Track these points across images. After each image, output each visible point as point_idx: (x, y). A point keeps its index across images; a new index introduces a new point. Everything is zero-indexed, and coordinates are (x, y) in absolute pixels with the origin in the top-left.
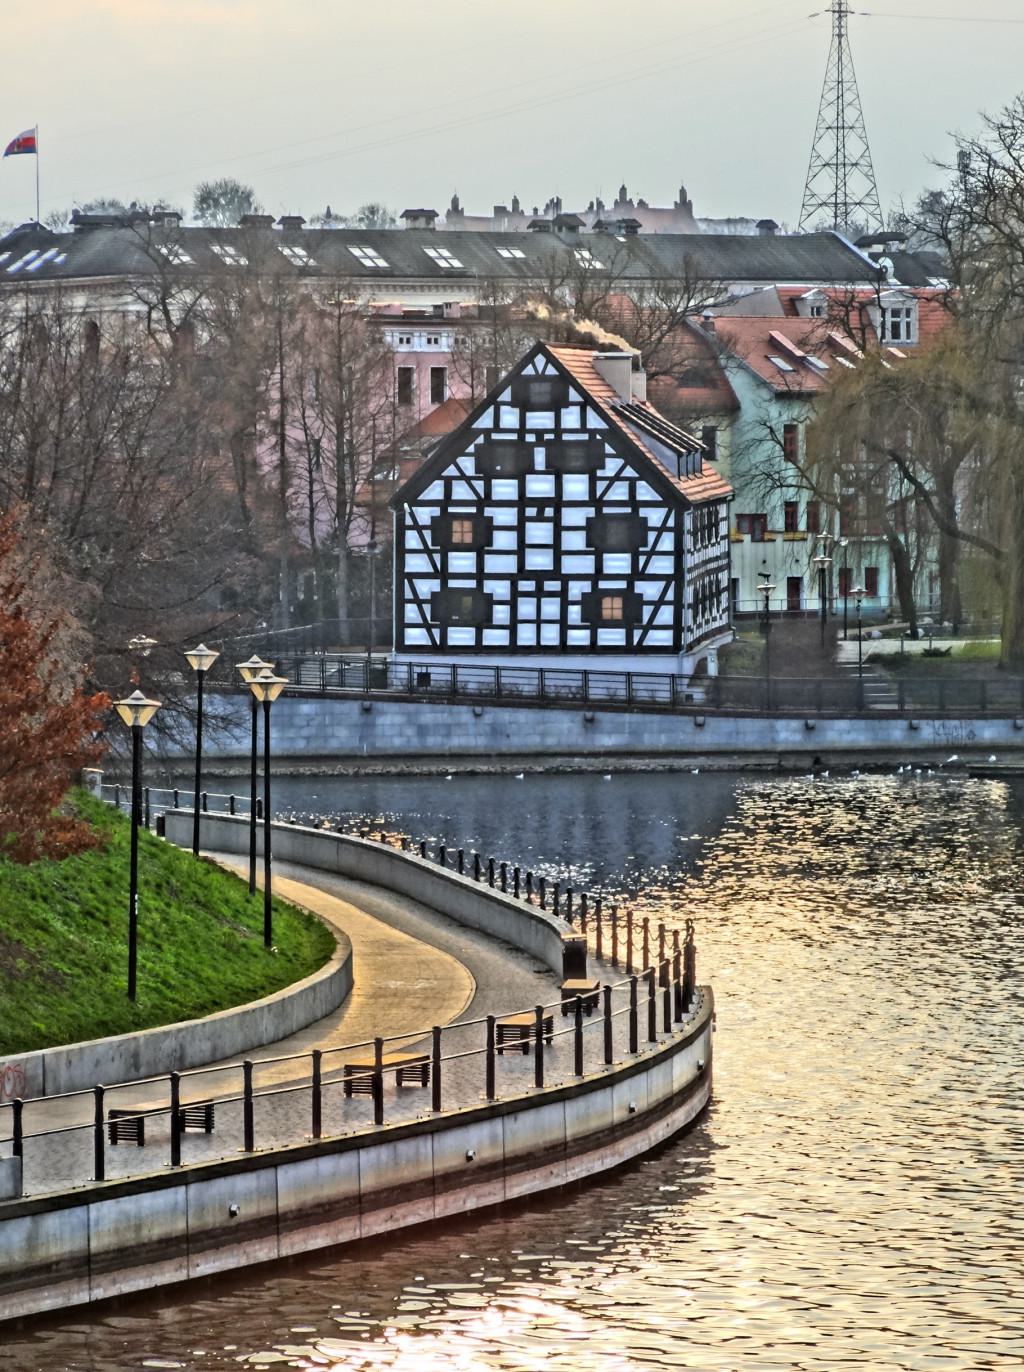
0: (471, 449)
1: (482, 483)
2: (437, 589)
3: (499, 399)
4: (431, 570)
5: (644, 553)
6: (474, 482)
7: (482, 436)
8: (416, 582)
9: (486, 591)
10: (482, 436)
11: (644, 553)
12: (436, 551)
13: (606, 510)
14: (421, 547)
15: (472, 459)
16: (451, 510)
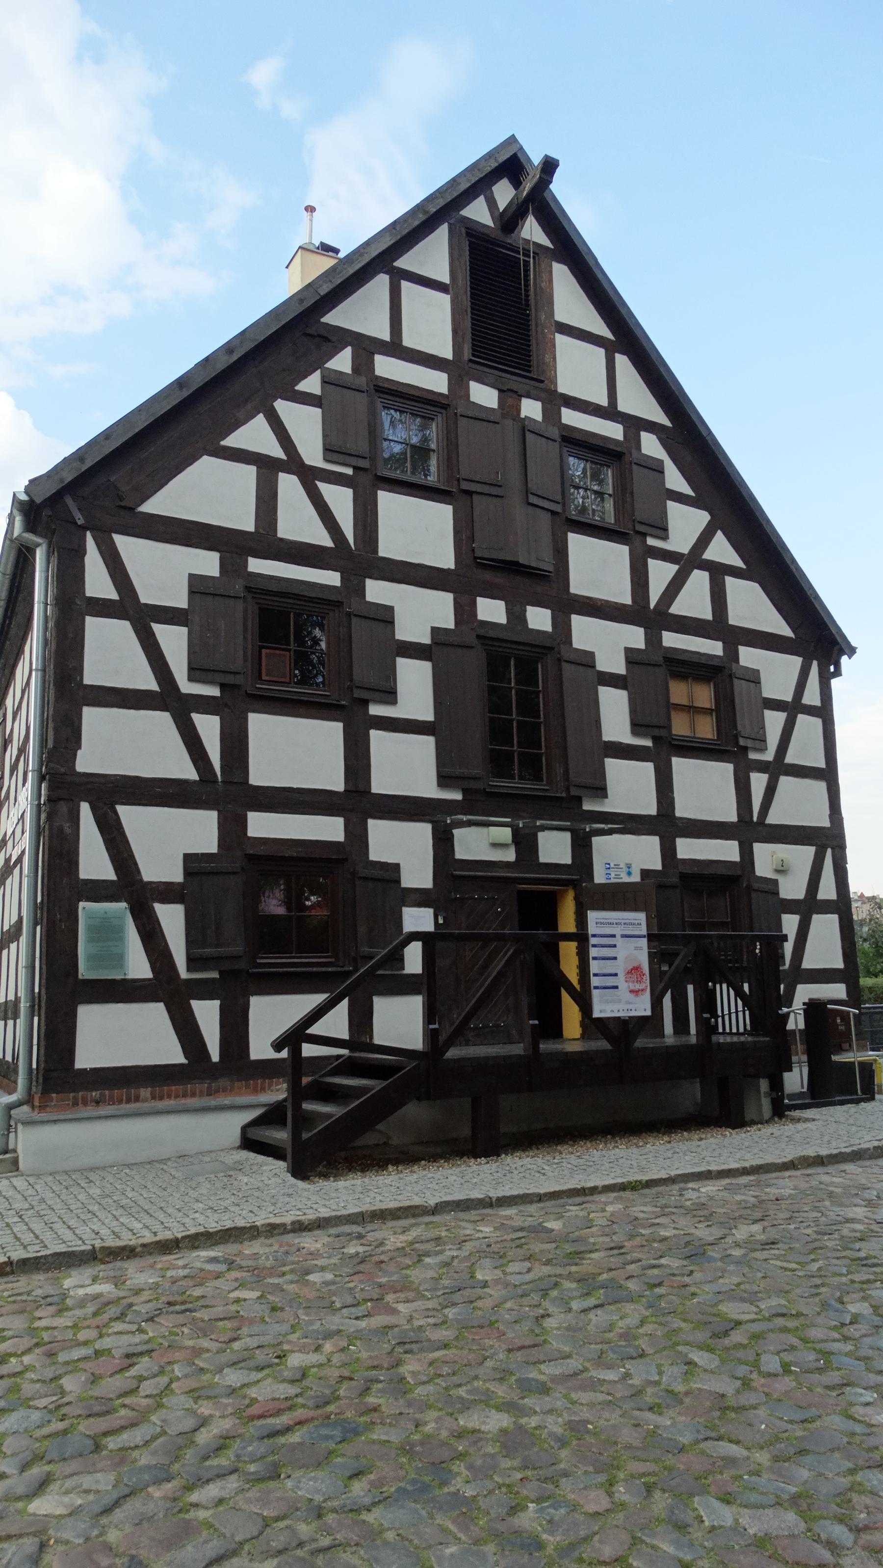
0: (312, 384)
1: (349, 492)
2: (212, 847)
3: (403, 263)
4: (190, 773)
5: (762, 767)
6: (326, 490)
7: (347, 352)
8: (129, 815)
9: (376, 854)
10: (347, 352)
11: (762, 767)
12: (206, 705)
13: (671, 640)
14: (148, 682)
15: (316, 413)
16: (257, 566)
